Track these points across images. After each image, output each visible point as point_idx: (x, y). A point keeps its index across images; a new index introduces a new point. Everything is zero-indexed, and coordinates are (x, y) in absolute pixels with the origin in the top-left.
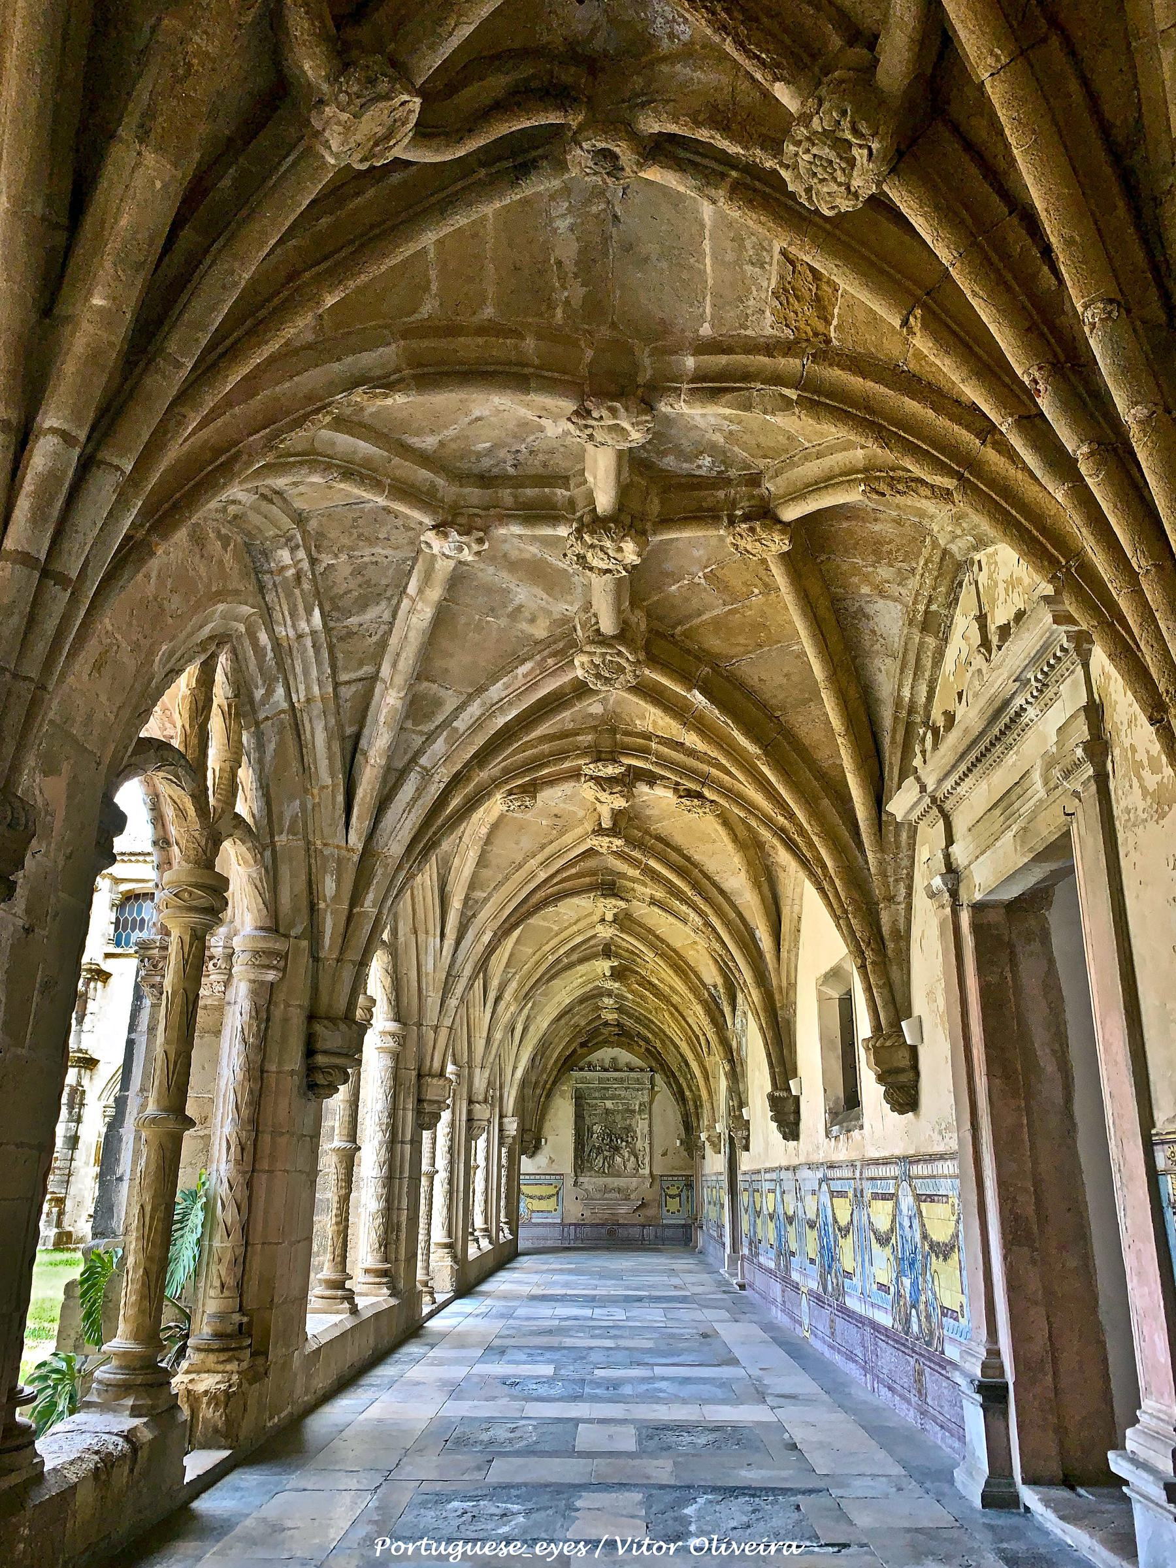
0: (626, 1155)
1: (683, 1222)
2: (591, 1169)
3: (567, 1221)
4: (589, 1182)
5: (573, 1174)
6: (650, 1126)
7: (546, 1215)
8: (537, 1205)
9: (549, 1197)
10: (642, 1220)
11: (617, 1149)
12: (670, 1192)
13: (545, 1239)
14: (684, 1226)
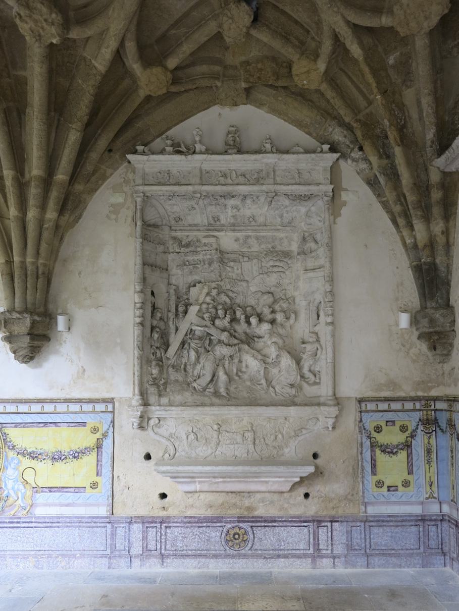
0: (272, 352)
1: (417, 510)
2: (187, 385)
3: (120, 512)
5: (136, 400)
6: (331, 280)
7: (69, 497)
8: (47, 474)
9: (77, 455)
10: (311, 508)
11: (250, 340)
12: (382, 439)
14: (422, 520)
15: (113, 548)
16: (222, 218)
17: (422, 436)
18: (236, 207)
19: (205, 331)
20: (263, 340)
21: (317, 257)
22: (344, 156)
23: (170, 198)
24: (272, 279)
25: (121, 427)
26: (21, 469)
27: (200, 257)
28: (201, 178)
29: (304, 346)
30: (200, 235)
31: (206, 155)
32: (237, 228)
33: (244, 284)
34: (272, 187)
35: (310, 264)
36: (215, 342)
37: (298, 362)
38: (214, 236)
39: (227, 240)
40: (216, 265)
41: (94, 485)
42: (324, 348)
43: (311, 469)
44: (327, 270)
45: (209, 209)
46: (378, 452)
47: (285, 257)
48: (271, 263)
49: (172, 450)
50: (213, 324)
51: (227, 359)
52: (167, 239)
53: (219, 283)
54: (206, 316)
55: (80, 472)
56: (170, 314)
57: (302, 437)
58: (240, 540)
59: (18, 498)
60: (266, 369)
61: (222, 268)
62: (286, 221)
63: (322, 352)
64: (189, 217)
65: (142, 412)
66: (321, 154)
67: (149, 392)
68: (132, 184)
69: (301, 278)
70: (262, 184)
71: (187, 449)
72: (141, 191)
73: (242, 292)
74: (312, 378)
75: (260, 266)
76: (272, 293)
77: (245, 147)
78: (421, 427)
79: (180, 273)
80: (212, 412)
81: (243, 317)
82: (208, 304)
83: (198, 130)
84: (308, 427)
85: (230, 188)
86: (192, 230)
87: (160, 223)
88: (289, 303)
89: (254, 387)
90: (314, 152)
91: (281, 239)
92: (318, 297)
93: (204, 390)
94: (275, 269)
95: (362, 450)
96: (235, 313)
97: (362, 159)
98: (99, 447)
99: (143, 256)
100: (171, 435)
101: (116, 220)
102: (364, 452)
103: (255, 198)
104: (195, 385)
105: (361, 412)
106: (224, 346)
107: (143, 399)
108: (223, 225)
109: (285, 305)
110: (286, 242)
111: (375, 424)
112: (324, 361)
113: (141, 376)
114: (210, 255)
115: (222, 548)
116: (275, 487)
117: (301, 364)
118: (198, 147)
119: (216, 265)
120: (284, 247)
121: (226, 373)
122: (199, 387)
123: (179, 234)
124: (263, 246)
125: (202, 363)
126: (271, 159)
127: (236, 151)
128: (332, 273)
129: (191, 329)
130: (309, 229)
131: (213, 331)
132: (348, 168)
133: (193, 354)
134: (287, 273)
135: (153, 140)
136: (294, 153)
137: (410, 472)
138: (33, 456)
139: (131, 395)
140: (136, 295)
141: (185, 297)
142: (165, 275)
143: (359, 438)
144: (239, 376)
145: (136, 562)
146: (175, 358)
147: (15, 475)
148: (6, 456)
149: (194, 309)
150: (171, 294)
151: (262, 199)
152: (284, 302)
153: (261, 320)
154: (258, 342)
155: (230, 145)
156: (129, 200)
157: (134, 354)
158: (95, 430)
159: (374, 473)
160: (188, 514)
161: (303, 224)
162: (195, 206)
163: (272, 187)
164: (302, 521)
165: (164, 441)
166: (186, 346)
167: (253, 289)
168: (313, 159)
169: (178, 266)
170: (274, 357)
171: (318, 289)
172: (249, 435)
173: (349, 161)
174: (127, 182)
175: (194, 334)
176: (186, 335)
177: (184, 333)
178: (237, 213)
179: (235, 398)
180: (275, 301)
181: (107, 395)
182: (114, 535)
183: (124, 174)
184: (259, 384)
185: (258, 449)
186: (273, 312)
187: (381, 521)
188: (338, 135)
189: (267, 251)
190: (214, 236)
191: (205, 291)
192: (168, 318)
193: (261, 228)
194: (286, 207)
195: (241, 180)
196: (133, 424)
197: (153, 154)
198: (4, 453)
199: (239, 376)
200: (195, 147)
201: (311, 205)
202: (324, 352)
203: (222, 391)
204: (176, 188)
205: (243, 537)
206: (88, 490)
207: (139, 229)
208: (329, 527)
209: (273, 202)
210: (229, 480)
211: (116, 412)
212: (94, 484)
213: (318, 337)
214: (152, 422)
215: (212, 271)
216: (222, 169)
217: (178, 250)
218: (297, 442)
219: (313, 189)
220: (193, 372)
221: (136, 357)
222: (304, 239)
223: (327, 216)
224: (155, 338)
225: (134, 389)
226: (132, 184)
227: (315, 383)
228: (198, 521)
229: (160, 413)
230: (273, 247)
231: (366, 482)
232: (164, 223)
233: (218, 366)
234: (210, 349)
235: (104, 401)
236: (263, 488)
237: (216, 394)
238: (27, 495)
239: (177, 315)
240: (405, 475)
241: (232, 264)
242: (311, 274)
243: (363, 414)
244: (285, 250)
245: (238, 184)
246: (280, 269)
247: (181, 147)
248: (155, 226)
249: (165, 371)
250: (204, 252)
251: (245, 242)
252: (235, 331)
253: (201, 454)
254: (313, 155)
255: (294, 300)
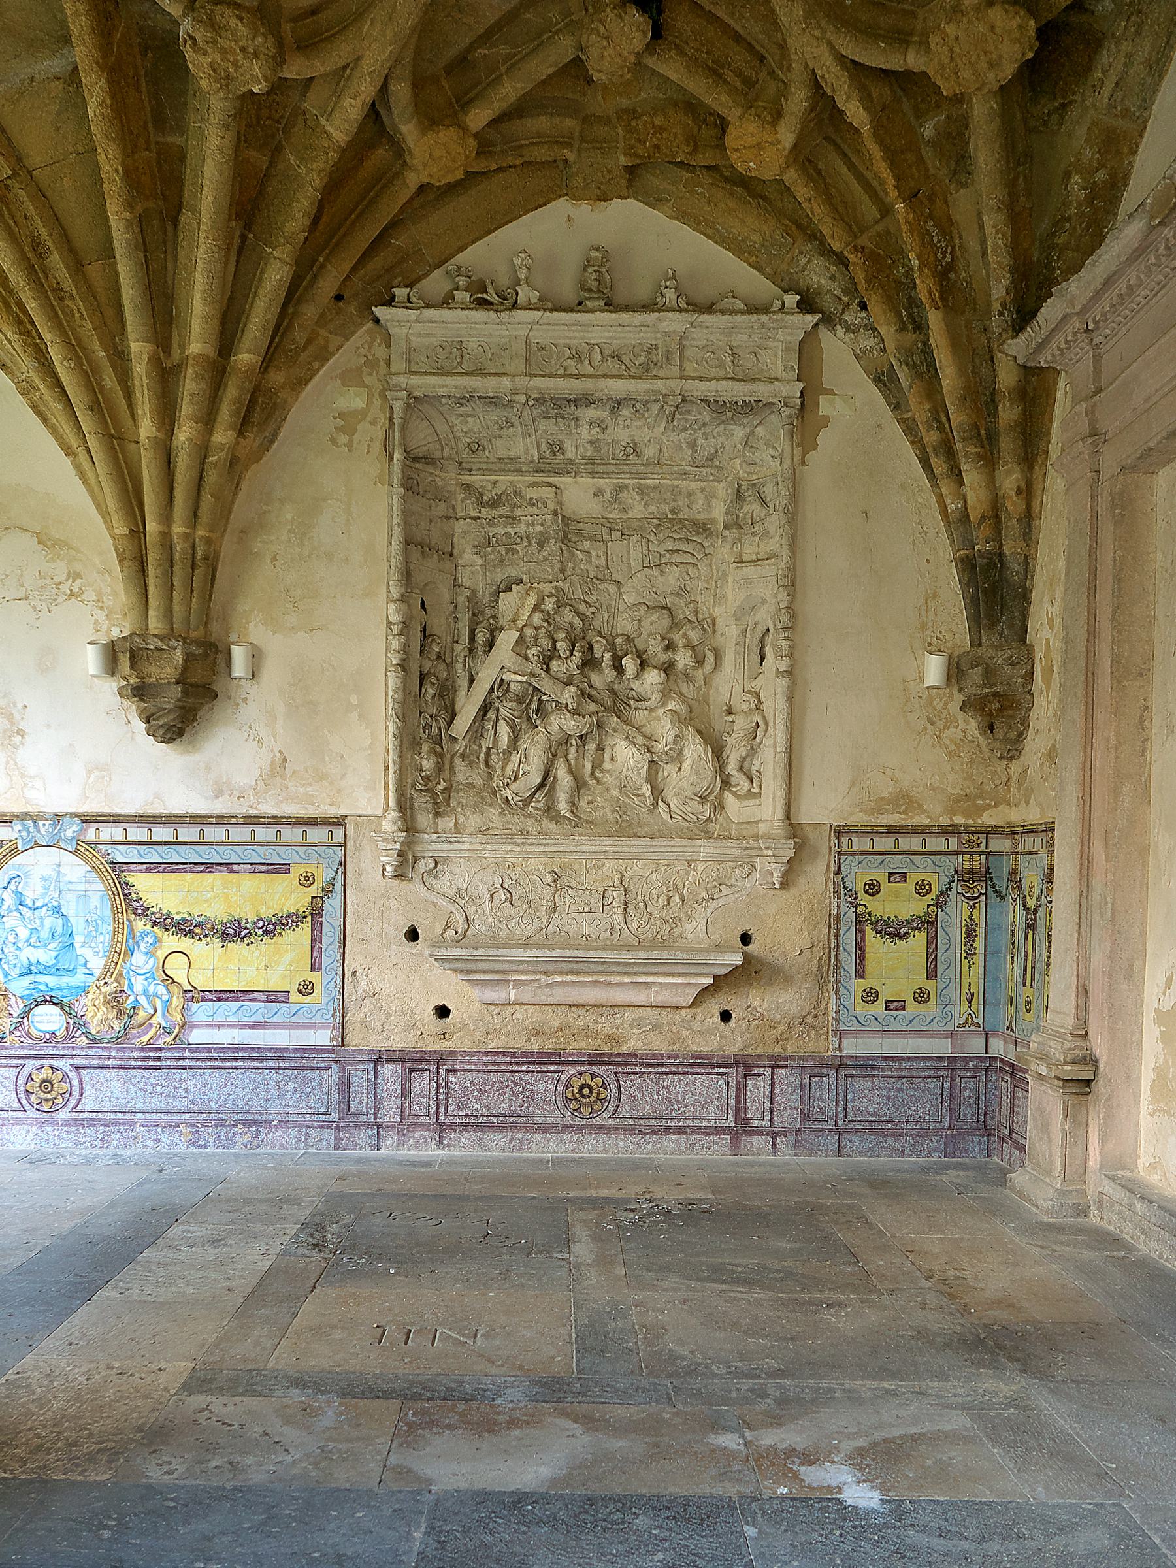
1: (941, 1047)
4: (475, 862)
5: (390, 823)
6: (792, 584)
7: (257, 1011)
8: (211, 965)
9: (271, 928)
10: (734, 1040)
11: (619, 704)
12: (879, 907)
13: (257, 1122)
14: (951, 1066)
15: (344, 1108)
16: (569, 445)
17: (959, 904)
18: (601, 425)
19: (530, 684)
20: (648, 704)
21: (765, 535)
22: (828, 320)
23: (463, 401)
24: (672, 578)
25: (360, 874)
26: (161, 954)
27: (522, 529)
28: (528, 361)
29: (730, 718)
30: (521, 481)
31: (541, 313)
32: (600, 469)
33: (612, 589)
34: (676, 385)
35: (750, 549)
36: (550, 707)
37: (718, 752)
38: (550, 485)
39: (580, 495)
40: (553, 546)
41: (306, 989)
42: (771, 724)
43: (738, 959)
44: (784, 562)
45: (542, 425)
46: (870, 932)
47: (698, 534)
48: (669, 545)
49: (461, 922)
50: (548, 671)
51: (573, 742)
52: (452, 489)
53: (561, 584)
54: (532, 652)
55: (279, 962)
56: (458, 648)
57: (722, 902)
58: (592, 1099)
59: (156, 1011)
60: (654, 766)
61: (566, 553)
62: (703, 455)
63: (766, 731)
64: (498, 443)
65: (402, 844)
66: (779, 316)
67: (416, 805)
68: (383, 368)
69: (730, 580)
70: (656, 377)
71: (490, 920)
72: (404, 386)
73: (609, 607)
74: (744, 784)
75: (645, 549)
76: (669, 609)
77: (620, 298)
78: (957, 887)
79: (480, 562)
80: (542, 848)
81: (607, 656)
82: (537, 629)
83: (523, 256)
84: (733, 882)
85: (588, 385)
86: (504, 470)
87: (438, 455)
88: (704, 630)
89: (626, 800)
90: (764, 309)
91: (690, 495)
92: (764, 617)
93: (527, 802)
94: (678, 558)
95: (838, 930)
96: (591, 647)
97: (866, 328)
98: (316, 913)
99: (406, 524)
100: (458, 892)
101: (349, 446)
102: (842, 932)
103: (637, 405)
104: (507, 793)
105: (839, 853)
106: (568, 715)
107: (404, 818)
108: (571, 462)
109: (694, 636)
110: (700, 502)
111: (867, 878)
112: (772, 750)
113: (401, 773)
114: (542, 525)
115: (557, 1113)
116: (664, 997)
117: (724, 755)
118: (524, 294)
119: (553, 546)
120: (697, 510)
121: (570, 771)
122: (517, 799)
123: (476, 479)
124: (653, 508)
125: (522, 749)
126: (675, 323)
127: (602, 303)
128: (793, 570)
129: (502, 680)
130: (748, 473)
131: (545, 685)
132: (836, 347)
133: (504, 730)
134: (702, 566)
135: (426, 275)
136: (723, 312)
137: (932, 975)
138: (185, 928)
139: (380, 812)
140: (391, 606)
141: (489, 613)
142: (448, 565)
143: (834, 905)
144: (596, 779)
145: (389, 1139)
146: (467, 740)
147: (149, 967)
148: (131, 929)
149: (507, 639)
150: (460, 605)
151: (655, 409)
152: (694, 629)
153: (643, 665)
154: (636, 709)
155: (590, 290)
156: (377, 402)
157: (386, 727)
158: (307, 880)
159: (860, 974)
160: (492, 1046)
161: (738, 462)
162: (515, 420)
163: (676, 385)
164: (712, 1063)
165: (444, 903)
166: (491, 714)
167: (629, 599)
168: (763, 326)
169: (474, 547)
170: (670, 740)
171: (764, 602)
172: (616, 896)
173: (840, 331)
174: (372, 364)
175: (508, 690)
176: (492, 690)
177: (488, 687)
178: (601, 436)
179: (587, 822)
180: (675, 625)
181: (331, 811)
182: (345, 1085)
183: (366, 346)
184: (638, 796)
185: (633, 922)
186: (670, 647)
187: (869, 1067)
188: (818, 274)
189: (660, 520)
190: (550, 485)
191: (532, 600)
192: (454, 659)
193: (649, 469)
194: (704, 425)
195: (612, 366)
196: (384, 869)
197: (429, 306)
198: (126, 923)
199: (596, 779)
200: (517, 294)
201: (755, 423)
202: (771, 731)
203: (563, 807)
204: (475, 382)
205: (599, 1094)
206: (295, 997)
207: (397, 466)
208: (768, 1077)
209: (677, 416)
210: (573, 978)
211: (350, 844)
212: (306, 986)
213: (759, 700)
214: (422, 866)
215: (546, 559)
216: (572, 341)
217: (474, 514)
218: (709, 911)
219: (762, 391)
220: (503, 769)
221: (391, 734)
222: (739, 495)
223: (788, 449)
224: (429, 697)
225: (387, 799)
226: (383, 368)
227: (750, 795)
228: (515, 1061)
229: (439, 847)
230: (673, 511)
231: (842, 991)
232: (447, 453)
233: (555, 755)
234: (538, 722)
235: (326, 821)
236: (640, 997)
237: (550, 811)
238: (174, 1006)
239: (471, 650)
240: (921, 981)
241: (587, 545)
242: (750, 571)
243: (843, 858)
244: (698, 517)
245: (604, 376)
246: (688, 558)
247: (487, 292)
248: (429, 460)
249: (447, 766)
250: (529, 518)
251: (615, 499)
252: (591, 686)
253: (519, 931)
254: (764, 318)
255: (714, 625)
